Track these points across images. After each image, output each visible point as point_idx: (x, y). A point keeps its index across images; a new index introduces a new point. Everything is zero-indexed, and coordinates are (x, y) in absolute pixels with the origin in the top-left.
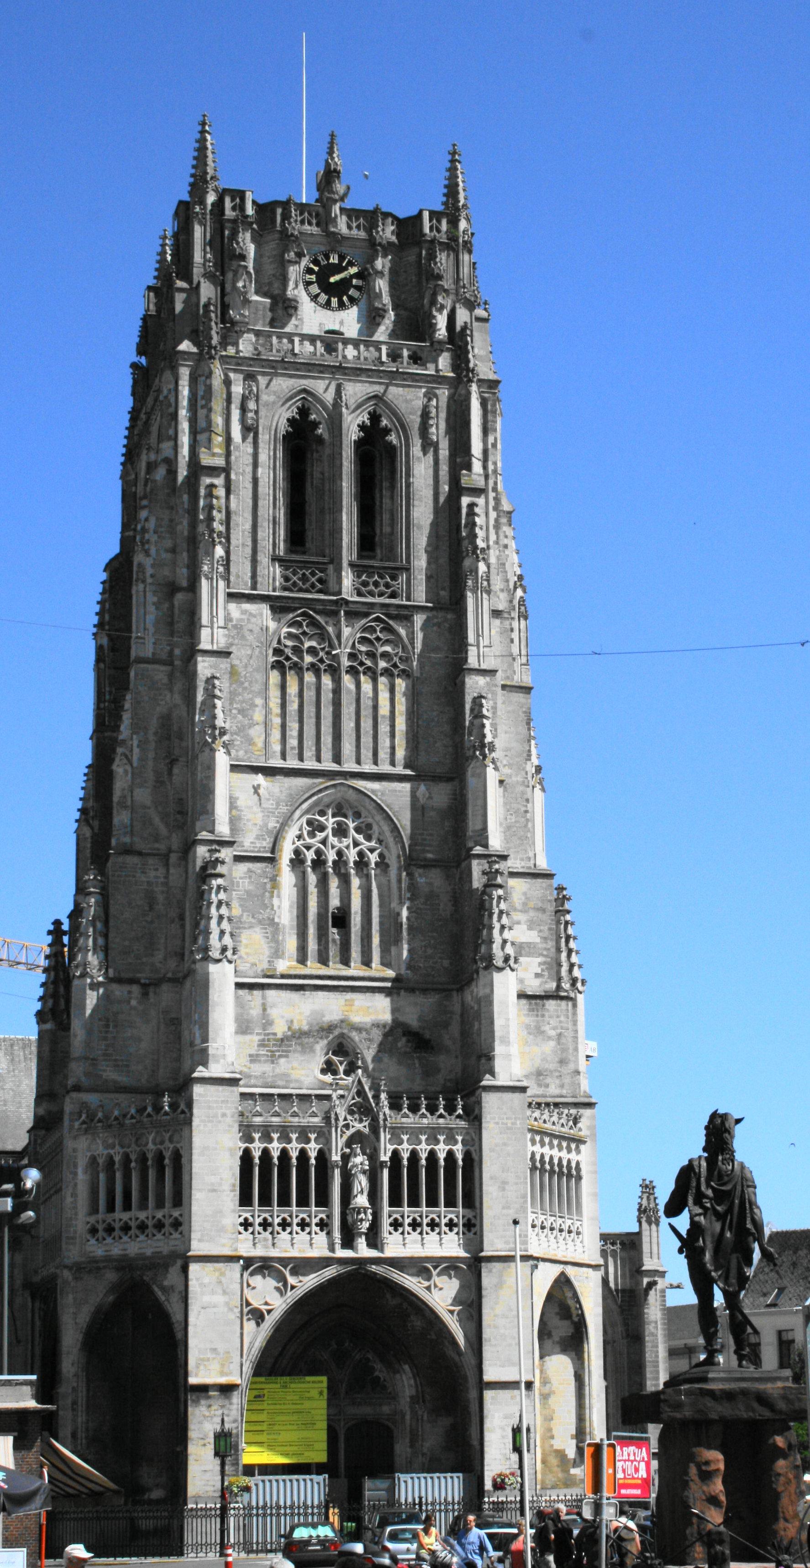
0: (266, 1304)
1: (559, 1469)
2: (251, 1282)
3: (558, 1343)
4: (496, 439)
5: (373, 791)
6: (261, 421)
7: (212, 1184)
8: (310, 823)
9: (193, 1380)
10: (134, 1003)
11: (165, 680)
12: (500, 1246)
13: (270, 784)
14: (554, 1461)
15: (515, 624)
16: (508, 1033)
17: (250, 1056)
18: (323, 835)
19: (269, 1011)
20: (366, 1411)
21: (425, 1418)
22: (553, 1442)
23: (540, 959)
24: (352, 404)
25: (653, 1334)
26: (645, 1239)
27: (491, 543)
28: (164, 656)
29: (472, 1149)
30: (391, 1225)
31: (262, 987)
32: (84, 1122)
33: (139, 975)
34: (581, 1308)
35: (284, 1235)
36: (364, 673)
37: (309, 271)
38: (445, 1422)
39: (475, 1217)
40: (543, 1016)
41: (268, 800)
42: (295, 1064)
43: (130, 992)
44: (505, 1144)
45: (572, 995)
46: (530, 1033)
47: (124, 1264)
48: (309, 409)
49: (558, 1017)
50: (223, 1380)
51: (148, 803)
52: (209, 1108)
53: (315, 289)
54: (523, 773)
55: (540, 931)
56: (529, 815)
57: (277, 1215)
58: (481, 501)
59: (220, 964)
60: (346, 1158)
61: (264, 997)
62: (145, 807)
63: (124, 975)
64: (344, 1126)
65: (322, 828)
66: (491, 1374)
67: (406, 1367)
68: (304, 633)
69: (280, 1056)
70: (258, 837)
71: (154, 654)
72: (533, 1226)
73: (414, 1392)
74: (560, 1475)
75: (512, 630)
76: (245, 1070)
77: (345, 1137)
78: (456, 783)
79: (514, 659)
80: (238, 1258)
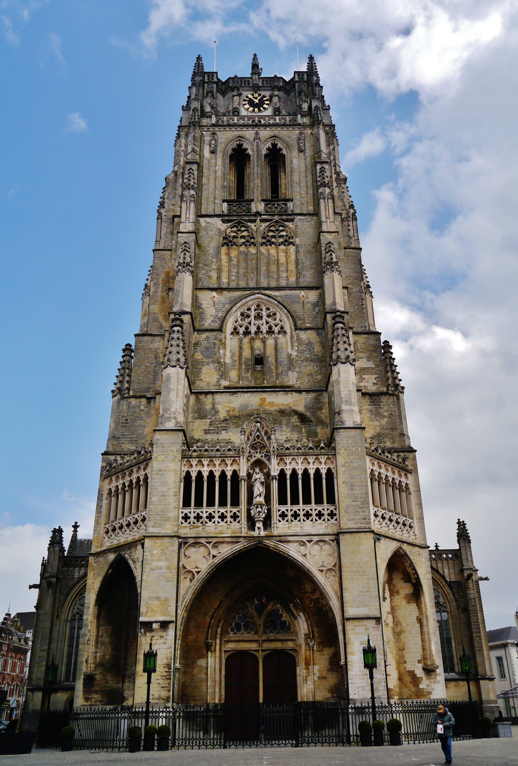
0: (197, 567)
1: (411, 686)
2: (186, 554)
3: (404, 598)
4: (334, 147)
5: (276, 296)
6: (218, 149)
7: (163, 492)
8: (242, 314)
9: (142, 619)
10: (142, 407)
11: (169, 257)
12: (351, 526)
13: (220, 297)
14: (408, 679)
15: (351, 223)
16: (351, 398)
17: (205, 430)
18: (250, 319)
19: (216, 406)
20: (278, 645)
21: (315, 648)
22: (405, 665)
23: (376, 376)
24: (263, 139)
25: (473, 606)
26: (463, 552)
27: (334, 187)
28: (169, 248)
29: (332, 467)
30: (280, 516)
31: (213, 393)
32: (108, 471)
33: (146, 394)
34: (416, 573)
35: (210, 524)
36: (271, 245)
37: (245, 100)
38: (328, 652)
39: (335, 509)
40: (379, 405)
41: (219, 303)
42: (231, 434)
43: (140, 402)
44: (351, 462)
45: (397, 393)
46: (372, 414)
47: (117, 549)
48: (242, 144)
49: (388, 405)
50: (161, 619)
51: (156, 311)
52: (163, 447)
53: (247, 106)
54: (359, 287)
55: (375, 361)
56: (364, 306)
57: (205, 511)
58: (326, 166)
59: (174, 368)
60: (249, 476)
61: (213, 399)
62: (154, 313)
63: (138, 394)
64: (249, 456)
65: (248, 316)
66: (350, 612)
67: (301, 614)
68: (239, 230)
69: (224, 430)
70: (213, 321)
71: (164, 247)
72: (376, 516)
73: (307, 632)
74: (413, 689)
75: (349, 226)
76: (202, 438)
77: (250, 463)
78: (320, 290)
79: (351, 238)
80: (179, 537)
